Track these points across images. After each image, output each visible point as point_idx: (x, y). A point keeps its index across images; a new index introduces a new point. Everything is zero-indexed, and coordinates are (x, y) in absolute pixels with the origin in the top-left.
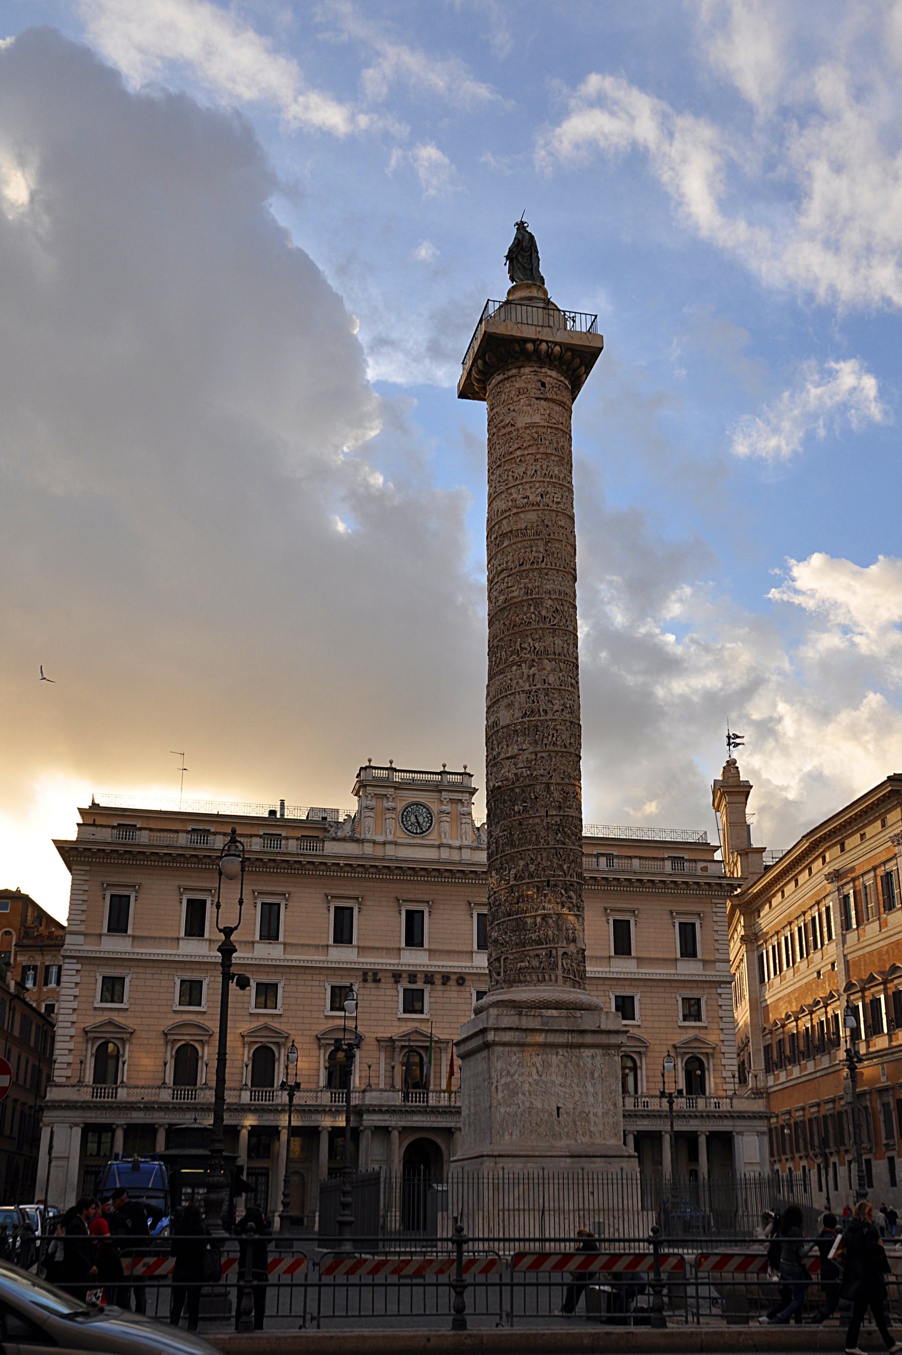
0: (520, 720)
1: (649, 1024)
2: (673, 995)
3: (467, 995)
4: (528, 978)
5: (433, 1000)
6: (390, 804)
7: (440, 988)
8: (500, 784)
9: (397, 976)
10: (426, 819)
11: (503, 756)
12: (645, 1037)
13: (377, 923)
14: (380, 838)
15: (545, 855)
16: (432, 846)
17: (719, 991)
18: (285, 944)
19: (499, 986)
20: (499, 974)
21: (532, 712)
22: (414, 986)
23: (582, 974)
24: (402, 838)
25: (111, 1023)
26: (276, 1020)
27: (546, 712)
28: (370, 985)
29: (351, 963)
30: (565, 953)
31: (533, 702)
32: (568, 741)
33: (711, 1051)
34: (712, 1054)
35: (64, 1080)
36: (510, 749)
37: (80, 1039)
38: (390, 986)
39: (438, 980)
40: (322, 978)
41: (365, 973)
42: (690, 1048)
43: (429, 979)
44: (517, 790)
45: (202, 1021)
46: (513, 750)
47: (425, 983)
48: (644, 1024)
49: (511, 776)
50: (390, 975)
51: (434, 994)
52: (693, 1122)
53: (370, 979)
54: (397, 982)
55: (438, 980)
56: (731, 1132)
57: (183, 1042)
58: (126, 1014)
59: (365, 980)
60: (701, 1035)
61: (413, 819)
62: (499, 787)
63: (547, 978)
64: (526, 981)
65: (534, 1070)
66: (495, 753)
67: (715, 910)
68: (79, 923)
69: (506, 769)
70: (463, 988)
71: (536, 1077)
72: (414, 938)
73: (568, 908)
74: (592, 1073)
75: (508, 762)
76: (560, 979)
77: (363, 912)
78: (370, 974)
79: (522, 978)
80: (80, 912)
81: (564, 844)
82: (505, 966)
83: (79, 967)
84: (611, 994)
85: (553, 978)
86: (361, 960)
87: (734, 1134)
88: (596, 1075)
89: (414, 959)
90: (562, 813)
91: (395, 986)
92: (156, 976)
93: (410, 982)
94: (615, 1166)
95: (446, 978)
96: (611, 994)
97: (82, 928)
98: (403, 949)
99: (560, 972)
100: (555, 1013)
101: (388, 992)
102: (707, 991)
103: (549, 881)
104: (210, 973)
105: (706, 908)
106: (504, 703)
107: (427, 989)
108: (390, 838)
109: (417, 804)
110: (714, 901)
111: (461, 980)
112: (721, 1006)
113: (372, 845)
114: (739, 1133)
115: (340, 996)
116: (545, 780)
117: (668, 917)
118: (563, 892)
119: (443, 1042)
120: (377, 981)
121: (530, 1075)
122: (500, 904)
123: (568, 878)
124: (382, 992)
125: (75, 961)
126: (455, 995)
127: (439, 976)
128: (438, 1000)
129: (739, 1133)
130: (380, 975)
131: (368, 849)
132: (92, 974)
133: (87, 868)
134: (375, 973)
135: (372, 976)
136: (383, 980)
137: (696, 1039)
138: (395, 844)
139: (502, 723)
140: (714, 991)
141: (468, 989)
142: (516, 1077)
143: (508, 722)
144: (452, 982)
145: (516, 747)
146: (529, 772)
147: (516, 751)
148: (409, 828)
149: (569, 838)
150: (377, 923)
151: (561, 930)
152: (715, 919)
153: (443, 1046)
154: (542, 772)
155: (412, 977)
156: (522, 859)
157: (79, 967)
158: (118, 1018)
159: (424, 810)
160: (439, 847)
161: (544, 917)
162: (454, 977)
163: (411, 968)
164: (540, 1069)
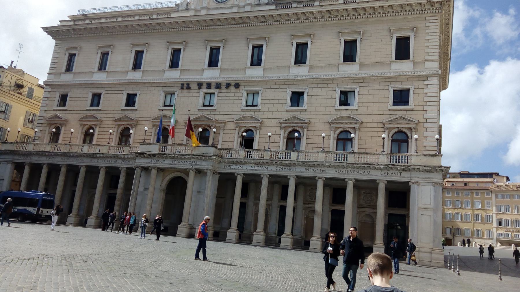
2: (387, 88)
3: (240, 94)
5: (220, 98)
7: (225, 91)
9: (200, 85)
12: (360, 118)
13: (195, 57)
16: (228, 8)
17: (426, 82)
18: (143, 71)
25: (57, 116)
26: (134, 112)
28: (185, 91)
29: (175, 79)
33: (414, 126)
34: (415, 129)
37: (46, 125)
38: (196, 91)
39: (224, 87)
40: (160, 88)
41: (183, 85)
42: (397, 123)
43: (218, 86)
47: (215, 88)
48: (361, 109)
50: (196, 85)
51: (221, 95)
52: (373, 172)
53: (185, 87)
55: (224, 87)
56: (408, 182)
59: (182, 88)
67: (428, 25)
70: (238, 90)
72: (213, 63)
77: (186, 51)
78: (185, 85)
83: (50, 90)
84: (337, 89)
86: (182, 77)
87: (410, 183)
89: (212, 75)
91: (198, 91)
93: (207, 88)
95: (228, 85)
96: (337, 89)
97: (54, 71)
98: (206, 69)
102: (415, 83)
104: (106, 89)
105: (421, 25)
107: (217, 91)
108: (205, 5)
111: (237, 86)
112: (427, 93)
113: (194, 11)
114: (415, 183)
117: (388, 34)
119: (221, 123)
125: (48, 87)
126: (233, 94)
127: (225, 84)
128: (223, 98)
129: (415, 183)
130: (191, 85)
131: (191, 13)
134: (188, 84)
135: (186, 86)
136: (192, 88)
138: (208, 9)
140: (422, 83)
141: (241, 91)
144: (232, 87)
150: (195, 57)
152: (427, 31)
153: (221, 125)
155: (209, 86)
157: (50, 90)
160: (231, 8)
162: (233, 84)
163: (208, 80)
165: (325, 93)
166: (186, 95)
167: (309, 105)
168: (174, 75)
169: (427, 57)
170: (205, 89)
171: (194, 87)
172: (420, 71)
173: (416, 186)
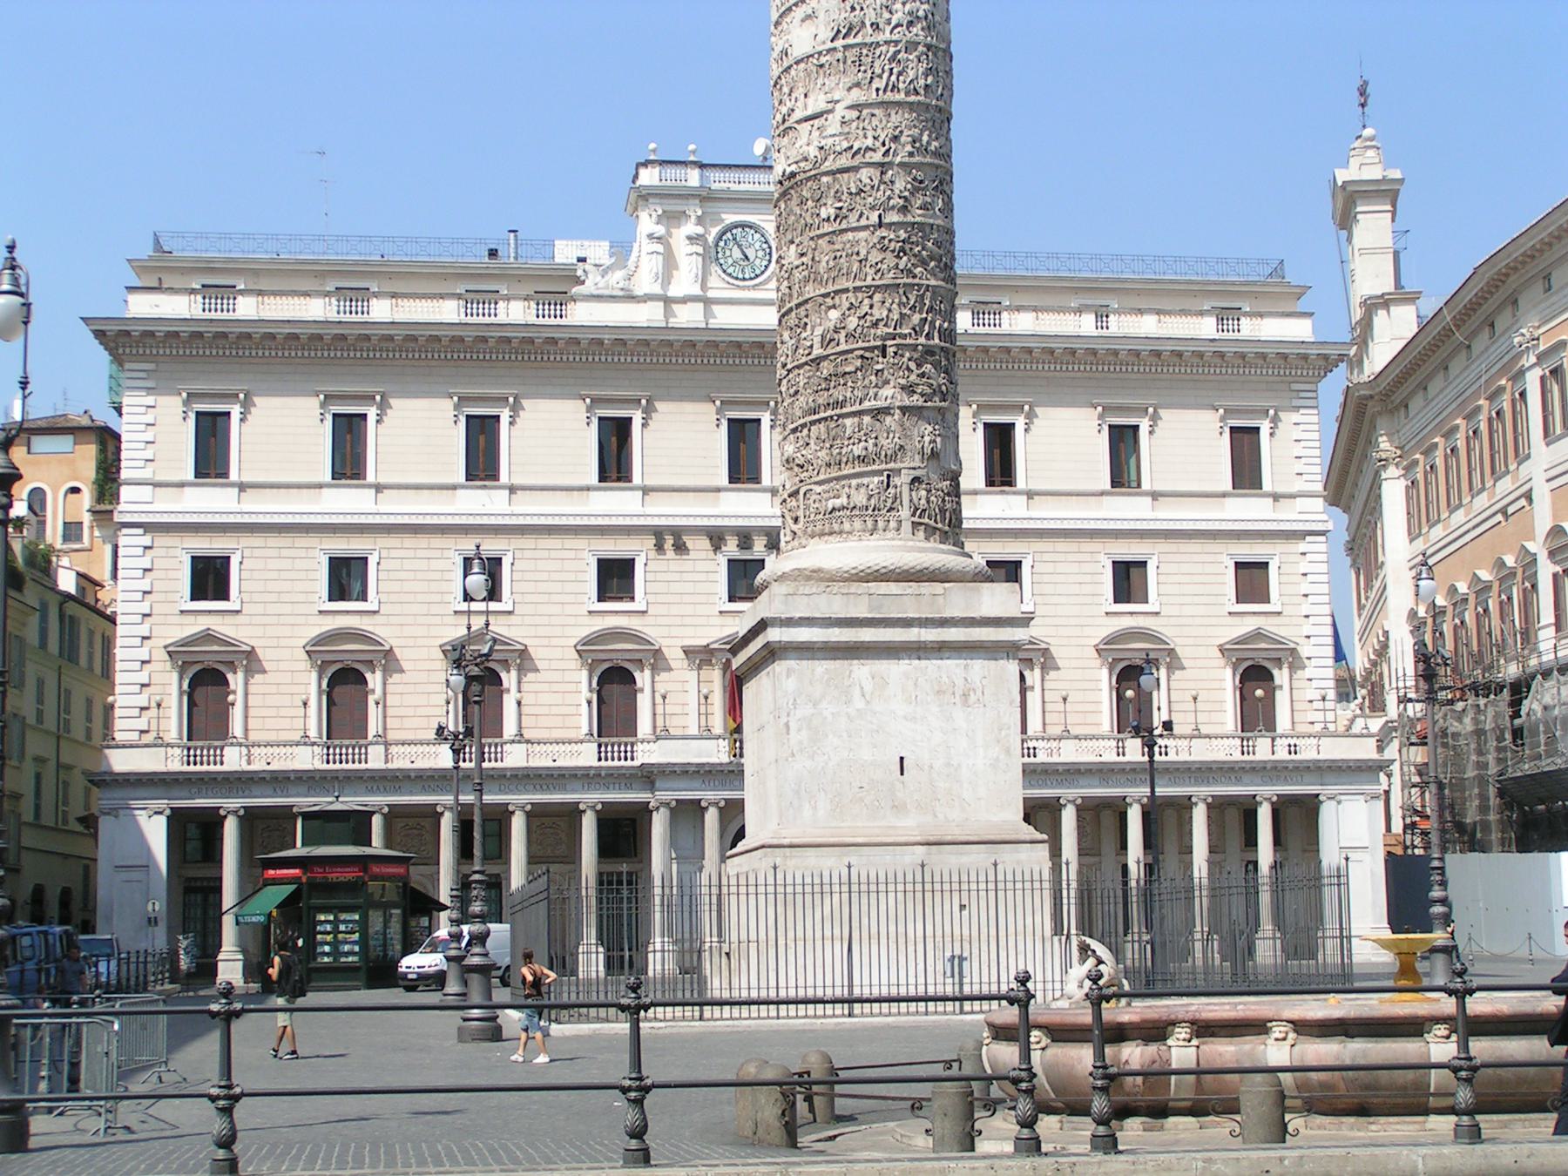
0: (829, 45)
1: (1174, 611)
4: (847, 526)
6: (691, 228)
8: (794, 168)
9: (716, 538)
10: (761, 254)
11: (798, 115)
14: (674, 291)
15: (877, 297)
17: (1302, 546)
19: (796, 542)
20: (796, 520)
21: (850, 29)
22: (747, 556)
23: (955, 520)
24: (718, 286)
27: (876, 26)
30: (916, 480)
31: (853, 9)
32: (922, 82)
35: (135, 736)
36: (810, 101)
38: (703, 555)
41: (658, 534)
44: (825, 179)
45: (370, 628)
46: (817, 103)
49: (813, 152)
54: (717, 548)
57: (339, 666)
58: (239, 619)
59: (659, 547)
60: (1271, 626)
61: (737, 254)
62: (793, 175)
63: (881, 524)
64: (841, 532)
65: (857, 692)
66: (784, 110)
68: (142, 463)
69: (805, 140)
71: (859, 704)
73: (922, 395)
74: (965, 695)
75: (807, 125)
76: (907, 526)
79: (836, 527)
80: (142, 445)
81: (915, 277)
82: (807, 507)
85: (893, 524)
88: (973, 698)
90: (909, 218)
92: (285, 553)
94: (1007, 856)
99: (905, 513)
100: (893, 588)
101: (701, 566)
103: (884, 347)
106: (799, 13)
109: (743, 225)
110: (1295, 387)
115: (615, 578)
116: (877, 157)
118: (912, 365)
120: (680, 548)
121: (848, 702)
122: (797, 392)
123: (922, 340)
124: (688, 566)
125: (140, 531)
132: (172, 552)
133: (151, 366)
135: (672, 539)
136: (689, 544)
137: (1258, 635)
139: (797, 52)
142: (824, 705)
143: (808, 50)
145: (822, 97)
146: (845, 145)
147: (823, 106)
148: (730, 270)
149: (924, 263)
151: (910, 437)
154: (869, 142)
155: (745, 538)
156: (834, 307)
157: (147, 540)
158: (224, 628)
159: (757, 236)
161: (878, 413)
164: (868, 687)
165: (1074, 568)
166: (674, 566)
167: (1039, 599)
168: (617, 504)
169: (1298, 485)
170: (731, 548)
171: (698, 545)
172: (1291, 515)
173: (1333, 803)
